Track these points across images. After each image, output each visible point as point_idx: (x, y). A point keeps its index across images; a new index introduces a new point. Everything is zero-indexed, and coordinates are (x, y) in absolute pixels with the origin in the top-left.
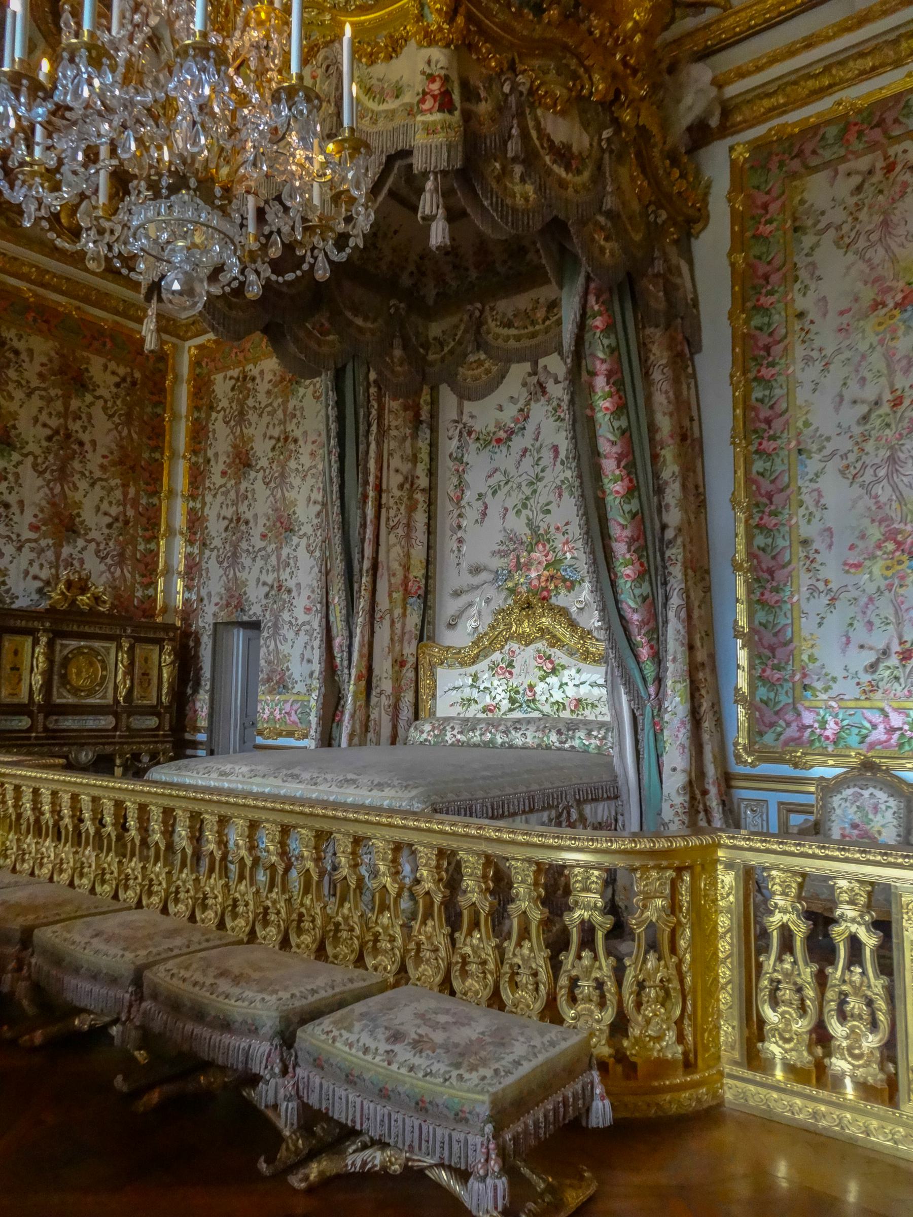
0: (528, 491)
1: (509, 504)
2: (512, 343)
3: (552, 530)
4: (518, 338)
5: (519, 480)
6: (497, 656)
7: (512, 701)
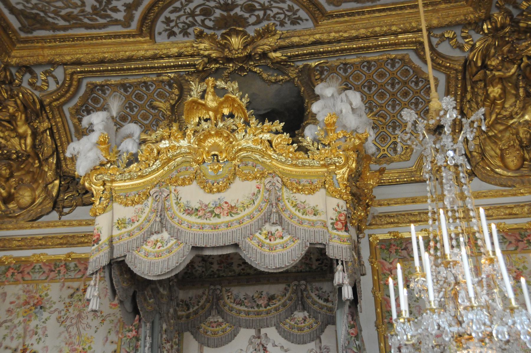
4: (248, 313)
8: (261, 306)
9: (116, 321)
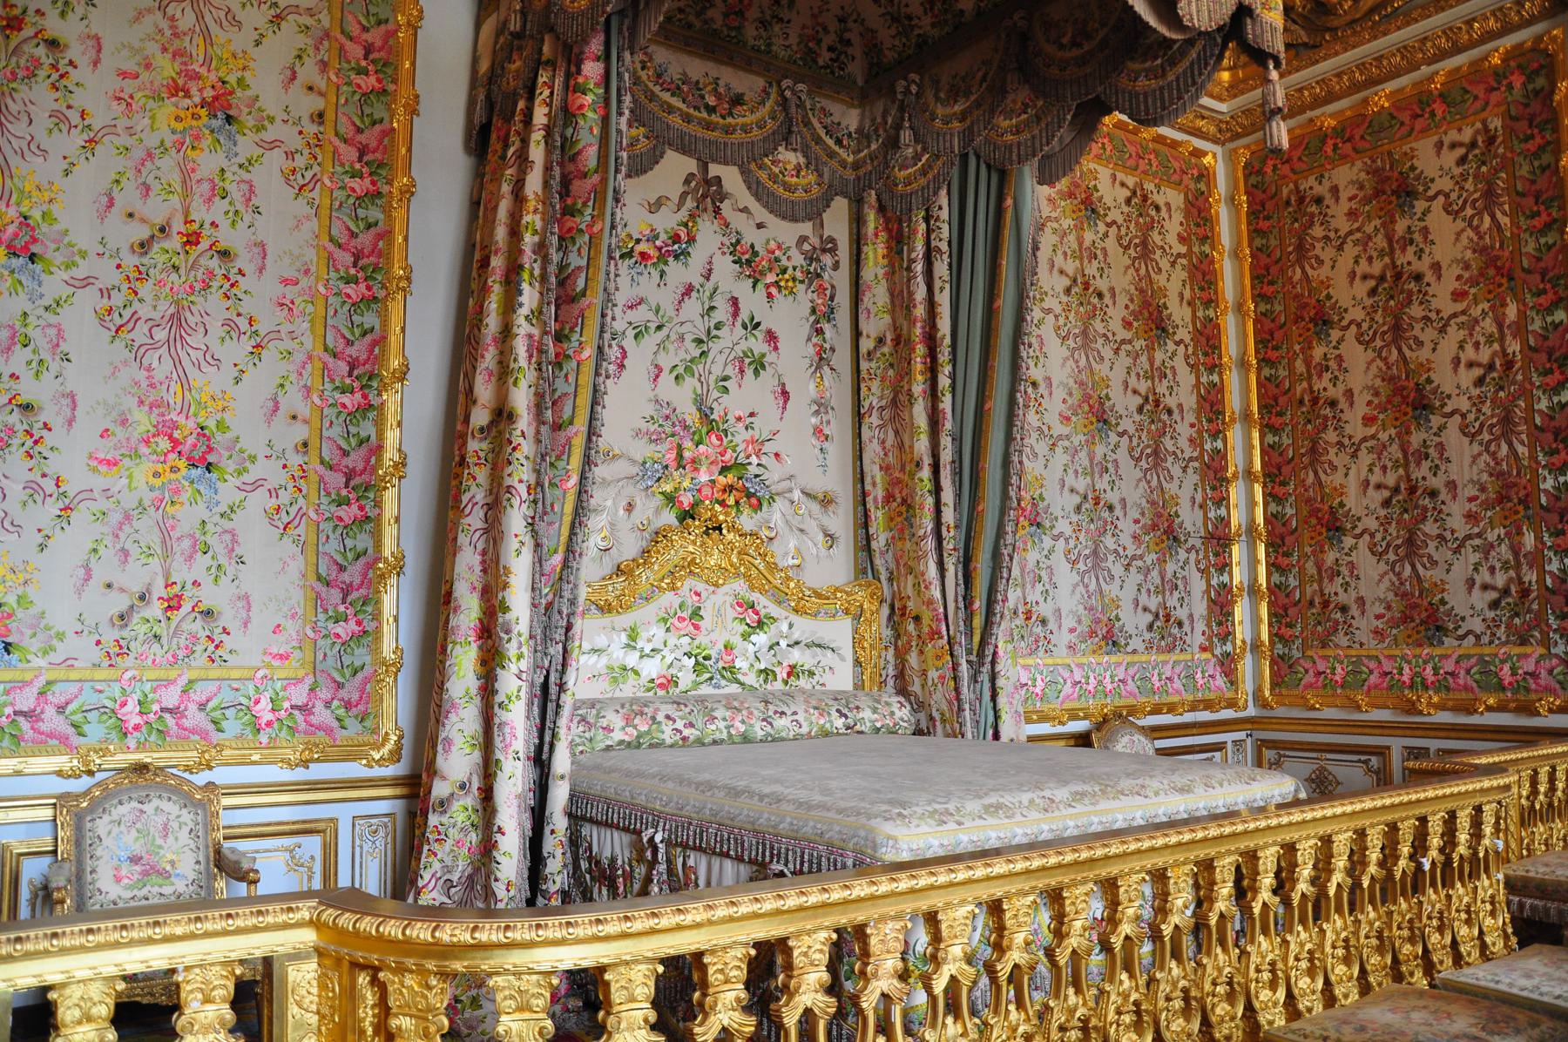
0: (697, 353)
1: (666, 361)
2: (676, 121)
3: (732, 420)
4: (687, 118)
5: (682, 330)
6: (668, 600)
7: (698, 668)
8: (711, 110)
9: (320, 34)
